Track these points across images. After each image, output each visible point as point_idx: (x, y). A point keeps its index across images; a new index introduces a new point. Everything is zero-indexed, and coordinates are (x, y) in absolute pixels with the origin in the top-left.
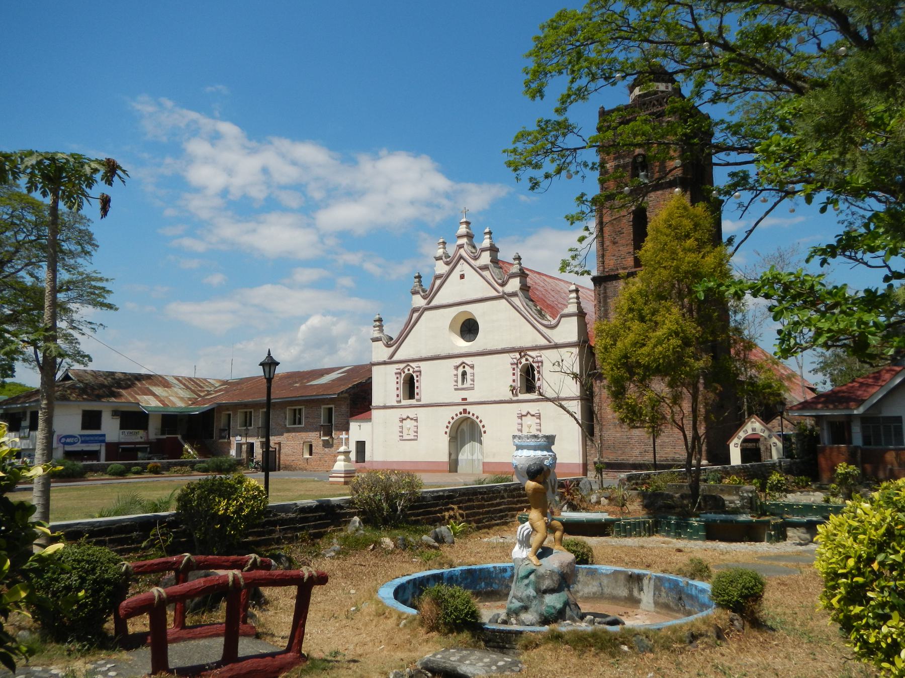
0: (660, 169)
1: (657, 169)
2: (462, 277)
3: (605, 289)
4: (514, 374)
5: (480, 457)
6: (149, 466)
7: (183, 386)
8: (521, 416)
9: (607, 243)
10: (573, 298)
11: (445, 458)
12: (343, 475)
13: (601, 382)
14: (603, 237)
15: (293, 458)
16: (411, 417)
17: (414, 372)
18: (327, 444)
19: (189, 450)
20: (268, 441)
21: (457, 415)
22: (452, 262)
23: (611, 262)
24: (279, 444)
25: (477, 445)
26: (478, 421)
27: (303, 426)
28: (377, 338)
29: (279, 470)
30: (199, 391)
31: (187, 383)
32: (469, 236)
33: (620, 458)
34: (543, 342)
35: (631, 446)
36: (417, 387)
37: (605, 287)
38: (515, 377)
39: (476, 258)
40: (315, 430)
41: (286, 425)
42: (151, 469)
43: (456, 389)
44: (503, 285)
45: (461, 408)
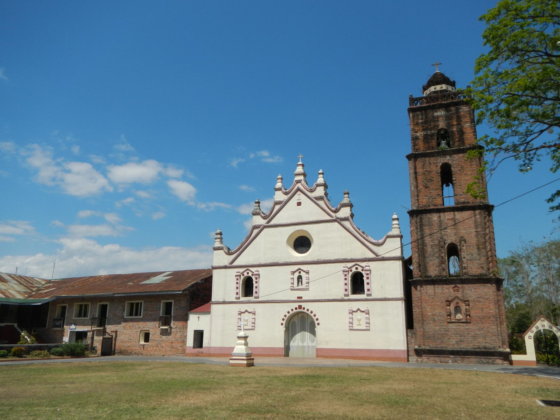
0: (459, 140)
1: (457, 139)
2: (299, 204)
3: (421, 219)
4: (346, 279)
5: (310, 344)
6: (13, 350)
7: (16, 282)
8: (352, 312)
9: (420, 187)
10: (396, 224)
11: (281, 345)
12: (245, 358)
13: (421, 287)
14: (417, 183)
15: (129, 344)
16: (249, 311)
17: (252, 275)
18: (165, 333)
19: (26, 337)
20: (105, 329)
21: (292, 310)
22: (290, 194)
23: (424, 201)
24: (116, 332)
25: (307, 335)
26: (312, 315)
27: (141, 317)
28: (219, 247)
29: (114, 355)
30: (31, 286)
31: (19, 280)
32: (304, 175)
33: (439, 346)
34: (372, 256)
35: (449, 336)
36: (256, 287)
37: (421, 218)
38: (346, 282)
39: (312, 191)
40: (154, 320)
41: (123, 316)
42: (15, 352)
43: (292, 290)
44: (336, 211)
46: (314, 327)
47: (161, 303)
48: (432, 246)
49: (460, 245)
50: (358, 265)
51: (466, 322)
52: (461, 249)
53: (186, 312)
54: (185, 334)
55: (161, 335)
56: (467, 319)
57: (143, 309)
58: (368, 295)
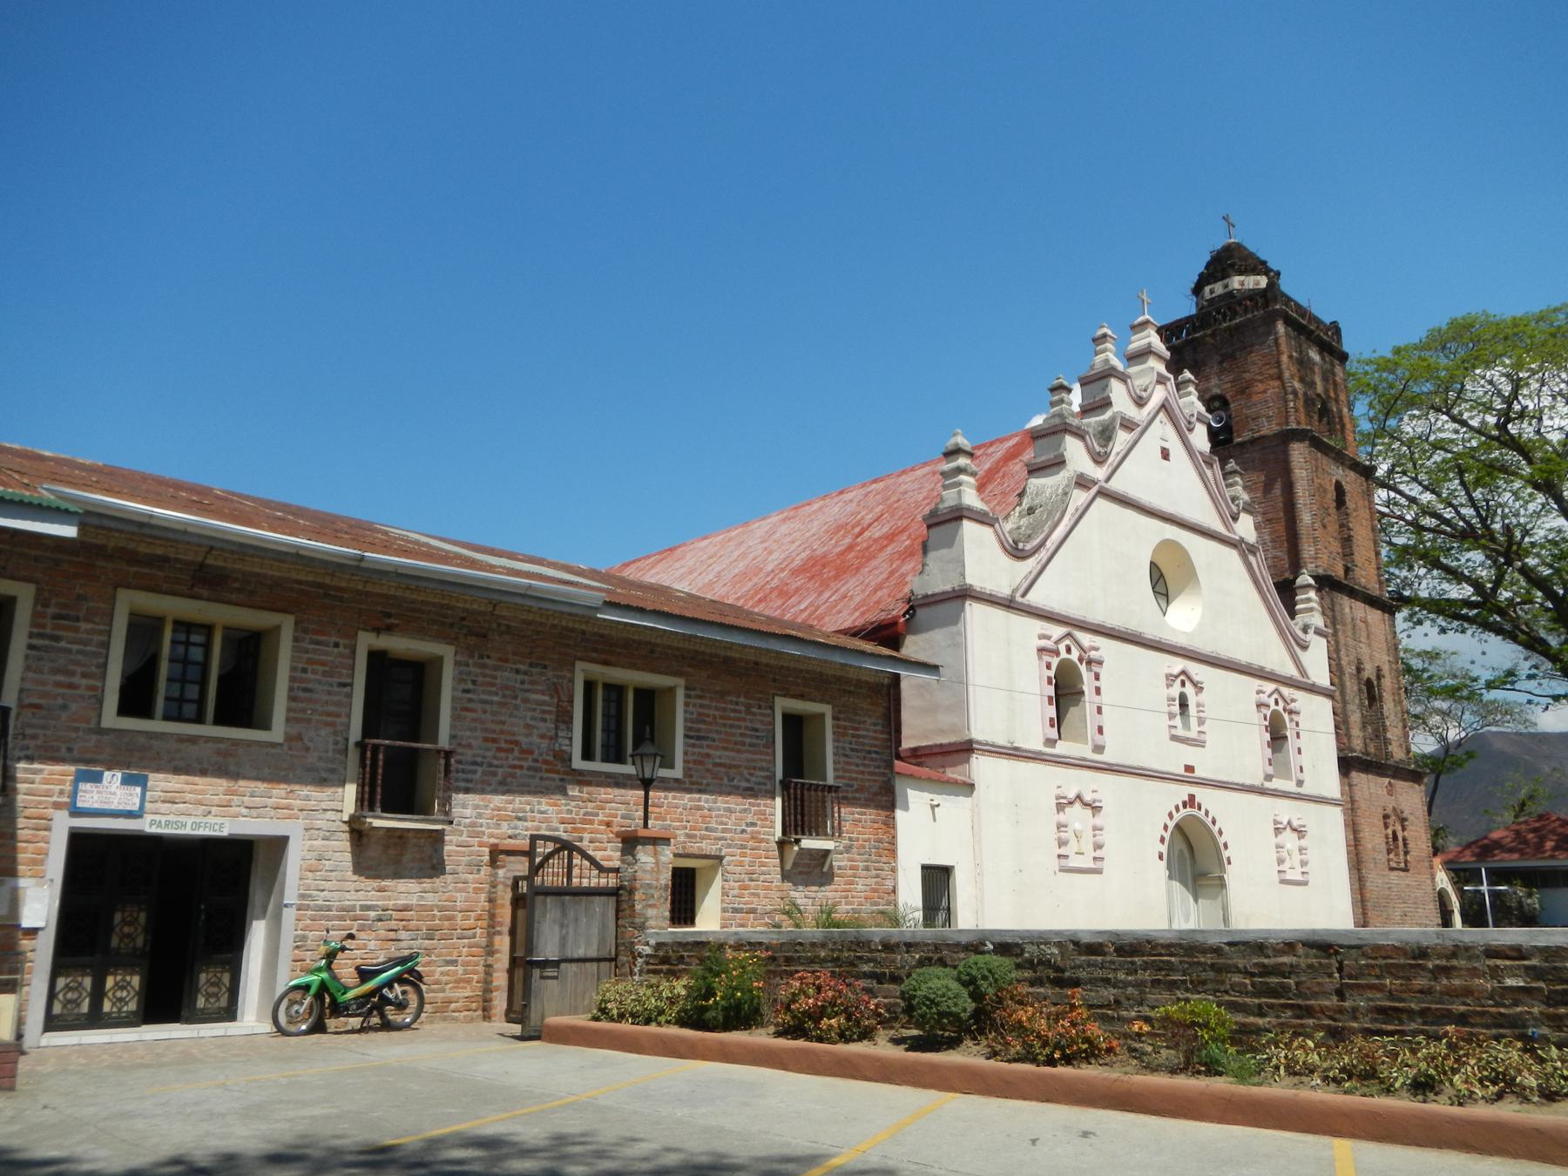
17: (1081, 660)
28: (985, 514)
45: (1183, 792)
46: (1222, 868)
47: (772, 708)
48: (1351, 674)
49: (1379, 686)
51: (1406, 870)
52: (1381, 697)
54: (889, 884)
56: (1406, 862)
57: (687, 728)
58: (1300, 783)
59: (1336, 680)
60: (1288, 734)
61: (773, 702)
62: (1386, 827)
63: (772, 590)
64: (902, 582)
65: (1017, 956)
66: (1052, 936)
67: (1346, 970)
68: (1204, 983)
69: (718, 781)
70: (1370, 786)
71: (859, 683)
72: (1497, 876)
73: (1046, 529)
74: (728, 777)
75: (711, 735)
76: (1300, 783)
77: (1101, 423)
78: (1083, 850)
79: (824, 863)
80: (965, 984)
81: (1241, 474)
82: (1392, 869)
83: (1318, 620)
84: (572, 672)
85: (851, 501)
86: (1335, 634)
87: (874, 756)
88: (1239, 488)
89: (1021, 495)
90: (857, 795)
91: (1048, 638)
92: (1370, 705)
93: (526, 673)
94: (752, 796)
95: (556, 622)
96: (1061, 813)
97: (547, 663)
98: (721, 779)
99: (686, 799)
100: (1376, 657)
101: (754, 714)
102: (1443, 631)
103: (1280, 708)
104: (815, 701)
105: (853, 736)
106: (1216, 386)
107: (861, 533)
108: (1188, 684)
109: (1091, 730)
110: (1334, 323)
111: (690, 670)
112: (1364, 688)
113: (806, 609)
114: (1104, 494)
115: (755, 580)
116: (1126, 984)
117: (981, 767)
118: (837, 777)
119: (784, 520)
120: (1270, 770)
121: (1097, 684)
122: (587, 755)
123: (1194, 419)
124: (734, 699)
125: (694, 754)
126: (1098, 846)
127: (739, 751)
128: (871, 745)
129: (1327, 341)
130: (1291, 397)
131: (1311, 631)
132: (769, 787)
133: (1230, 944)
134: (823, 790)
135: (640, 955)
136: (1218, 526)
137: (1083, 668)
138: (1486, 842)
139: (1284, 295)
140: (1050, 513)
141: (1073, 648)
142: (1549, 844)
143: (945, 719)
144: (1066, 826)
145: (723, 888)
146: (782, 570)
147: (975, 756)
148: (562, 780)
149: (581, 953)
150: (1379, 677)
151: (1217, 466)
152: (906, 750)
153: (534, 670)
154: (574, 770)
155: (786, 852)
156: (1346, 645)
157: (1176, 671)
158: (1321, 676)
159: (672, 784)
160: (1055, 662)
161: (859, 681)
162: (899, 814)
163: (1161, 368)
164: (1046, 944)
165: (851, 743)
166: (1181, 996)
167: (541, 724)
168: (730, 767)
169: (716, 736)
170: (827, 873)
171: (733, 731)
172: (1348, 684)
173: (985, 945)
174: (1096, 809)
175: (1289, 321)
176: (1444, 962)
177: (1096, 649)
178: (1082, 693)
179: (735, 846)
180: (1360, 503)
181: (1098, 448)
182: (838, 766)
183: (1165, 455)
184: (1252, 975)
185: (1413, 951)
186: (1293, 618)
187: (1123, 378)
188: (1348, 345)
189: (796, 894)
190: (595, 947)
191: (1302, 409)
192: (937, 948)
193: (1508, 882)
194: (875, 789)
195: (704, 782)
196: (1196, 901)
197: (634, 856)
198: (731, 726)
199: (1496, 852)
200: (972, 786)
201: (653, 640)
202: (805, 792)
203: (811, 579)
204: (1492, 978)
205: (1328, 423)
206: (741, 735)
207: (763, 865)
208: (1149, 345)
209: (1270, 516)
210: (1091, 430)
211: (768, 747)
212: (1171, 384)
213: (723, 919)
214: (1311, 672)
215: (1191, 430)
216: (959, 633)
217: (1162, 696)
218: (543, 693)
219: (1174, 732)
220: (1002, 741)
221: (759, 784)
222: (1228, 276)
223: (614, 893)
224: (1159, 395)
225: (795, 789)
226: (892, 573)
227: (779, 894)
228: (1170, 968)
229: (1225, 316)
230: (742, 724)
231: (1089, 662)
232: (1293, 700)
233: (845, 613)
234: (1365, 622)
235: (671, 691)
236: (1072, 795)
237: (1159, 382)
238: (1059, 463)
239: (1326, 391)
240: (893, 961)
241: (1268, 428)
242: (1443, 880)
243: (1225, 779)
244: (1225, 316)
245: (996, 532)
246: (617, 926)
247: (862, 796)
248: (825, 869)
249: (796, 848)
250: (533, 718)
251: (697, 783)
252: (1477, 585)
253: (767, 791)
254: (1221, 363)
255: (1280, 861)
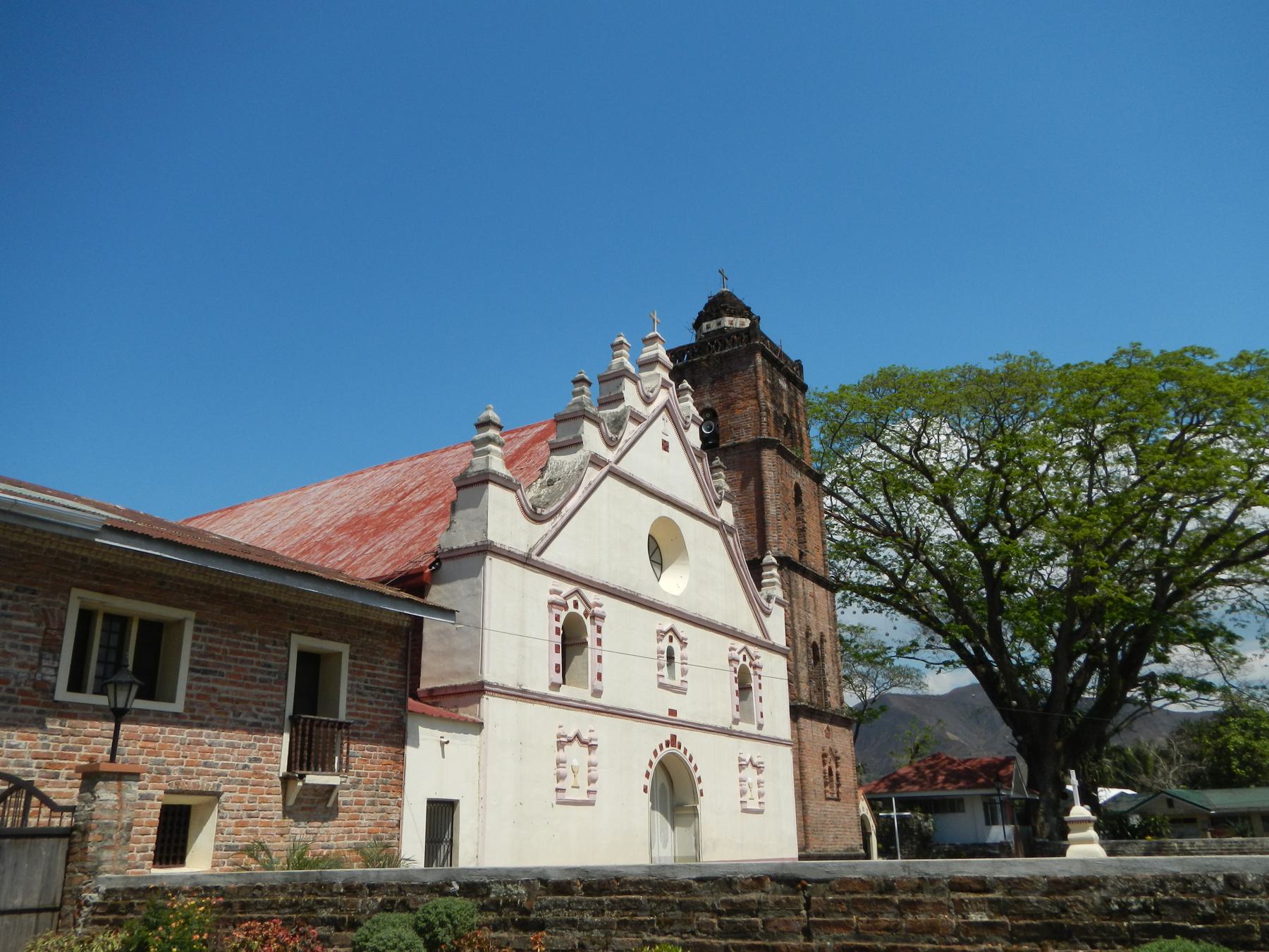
17: (586, 614)
21: (661, 747)
28: (510, 480)
41: (47, 689)
45: (666, 732)
46: (696, 800)
47: (288, 645)
49: (822, 648)
50: (747, 651)
51: (838, 800)
52: (823, 657)
53: (397, 712)
54: (394, 818)
55: (289, 821)
56: (838, 793)
57: (192, 662)
58: (760, 727)
59: (790, 643)
60: (752, 685)
61: (290, 639)
62: (824, 764)
63: (317, 543)
64: (433, 537)
65: (483, 897)
66: (521, 874)
67: (814, 906)
68: (671, 923)
69: (224, 717)
70: (814, 730)
71: (379, 625)
72: (904, 804)
73: (562, 499)
74: (234, 711)
75: (219, 669)
76: (760, 727)
77: (614, 415)
78: (579, 784)
79: (327, 800)
80: (421, 932)
81: (724, 469)
82: (828, 799)
83: (778, 593)
84: (67, 600)
85: (399, 471)
86: (791, 605)
87: (388, 694)
88: (723, 480)
89: (543, 470)
90: (368, 732)
91: (559, 593)
92: (815, 664)
93: (10, 598)
94: (258, 732)
95: (53, 547)
96: (561, 751)
97: (36, 588)
98: (226, 714)
99: (185, 734)
100: (820, 626)
101: (269, 650)
102: (866, 611)
103: (747, 663)
104: (332, 640)
105: (369, 675)
106: (710, 401)
107: (403, 498)
108: (674, 639)
109: (591, 676)
110: (798, 362)
111: (203, 603)
112: (811, 649)
113: (344, 560)
114: (614, 473)
115: (302, 535)
116: (593, 926)
117: (491, 707)
118: (349, 714)
119: (337, 486)
120: (737, 715)
121: (599, 636)
122: (76, 684)
123: (689, 420)
124: (249, 635)
125: (199, 688)
126: (592, 781)
127: (248, 686)
128: (387, 684)
129: (792, 374)
130: (765, 413)
131: (773, 601)
132: (277, 722)
133: (699, 880)
134: (333, 727)
135: (87, 904)
136: (705, 510)
137: (587, 622)
138: (895, 776)
139: (762, 334)
140: (567, 486)
141: (580, 604)
142: (941, 778)
143: (462, 662)
144: (564, 762)
145: (218, 826)
146: (328, 527)
147: (485, 696)
148: (40, 712)
149: (17, 903)
150: (822, 641)
151: (706, 460)
152: (423, 691)
153: (20, 595)
154: (56, 702)
155: (290, 790)
156: (799, 614)
157: (665, 628)
158: (779, 639)
159: (170, 718)
160: (563, 615)
161: (380, 623)
162: (409, 750)
163: (666, 375)
164: (513, 883)
165: (366, 682)
166: (646, 938)
167: (22, 652)
168: (238, 702)
169: (225, 671)
170: (332, 809)
171: (244, 666)
172: (799, 646)
173: (451, 886)
174: (592, 747)
175: (765, 355)
176: (909, 897)
177: (600, 605)
178: (586, 643)
179: (235, 782)
180: (812, 502)
181: (610, 435)
182: (352, 703)
183: (666, 446)
184: (720, 913)
185: (879, 885)
186: (759, 590)
187: (635, 380)
188: (807, 380)
189: (298, 830)
190: (36, 896)
191: (772, 424)
192: (401, 889)
193: (912, 810)
194: (387, 725)
195: (208, 716)
196: (673, 828)
197: (92, 793)
198: (242, 661)
199: (903, 784)
200: (481, 725)
201: (164, 572)
202: (315, 728)
203: (352, 535)
204: (957, 912)
205: (791, 438)
206: (252, 670)
207: (263, 801)
208: (657, 355)
209: (745, 507)
210: (605, 419)
211: (280, 684)
212: (673, 389)
213: (215, 857)
214: (771, 635)
215: (687, 429)
216: (478, 584)
217: (651, 647)
218: (29, 619)
219: (661, 680)
220: (511, 684)
221: (267, 719)
222: (721, 316)
223: (66, 833)
224: (662, 397)
225: (304, 725)
226: (425, 531)
227: (279, 830)
228: (637, 907)
229: (717, 346)
230: (255, 659)
231: (593, 617)
232: (757, 657)
233: (378, 565)
234: (813, 596)
235: (180, 623)
236: (571, 734)
237: (663, 386)
238: (577, 443)
239: (791, 413)
240: (354, 905)
241: (746, 437)
242: (864, 808)
243: (702, 722)
244: (717, 346)
245: (518, 496)
246: (66, 872)
247: (374, 733)
248: (330, 805)
249: (300, 784)
250: (13, 646)
251: (199, 718)
252: (892, 575)
253: (274, 727)
254: (713, 382)
255: (743, 793)
